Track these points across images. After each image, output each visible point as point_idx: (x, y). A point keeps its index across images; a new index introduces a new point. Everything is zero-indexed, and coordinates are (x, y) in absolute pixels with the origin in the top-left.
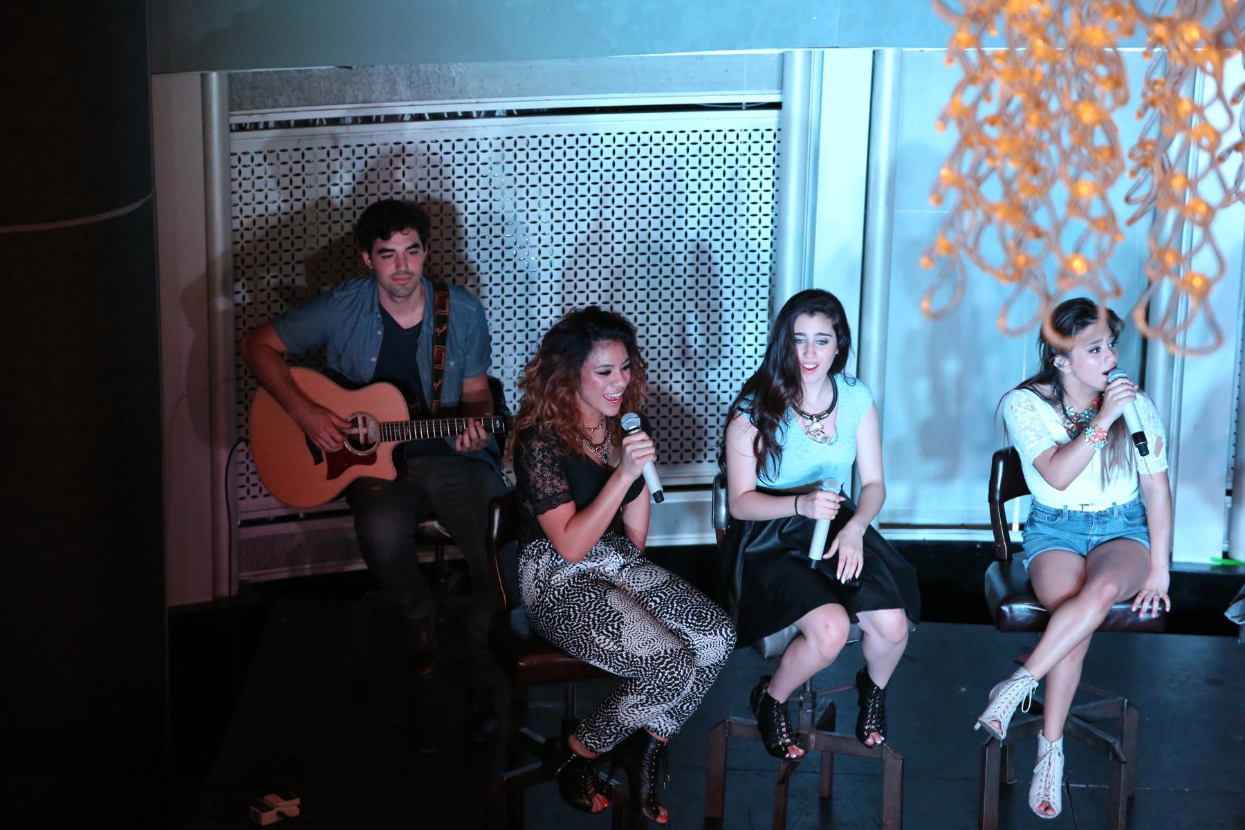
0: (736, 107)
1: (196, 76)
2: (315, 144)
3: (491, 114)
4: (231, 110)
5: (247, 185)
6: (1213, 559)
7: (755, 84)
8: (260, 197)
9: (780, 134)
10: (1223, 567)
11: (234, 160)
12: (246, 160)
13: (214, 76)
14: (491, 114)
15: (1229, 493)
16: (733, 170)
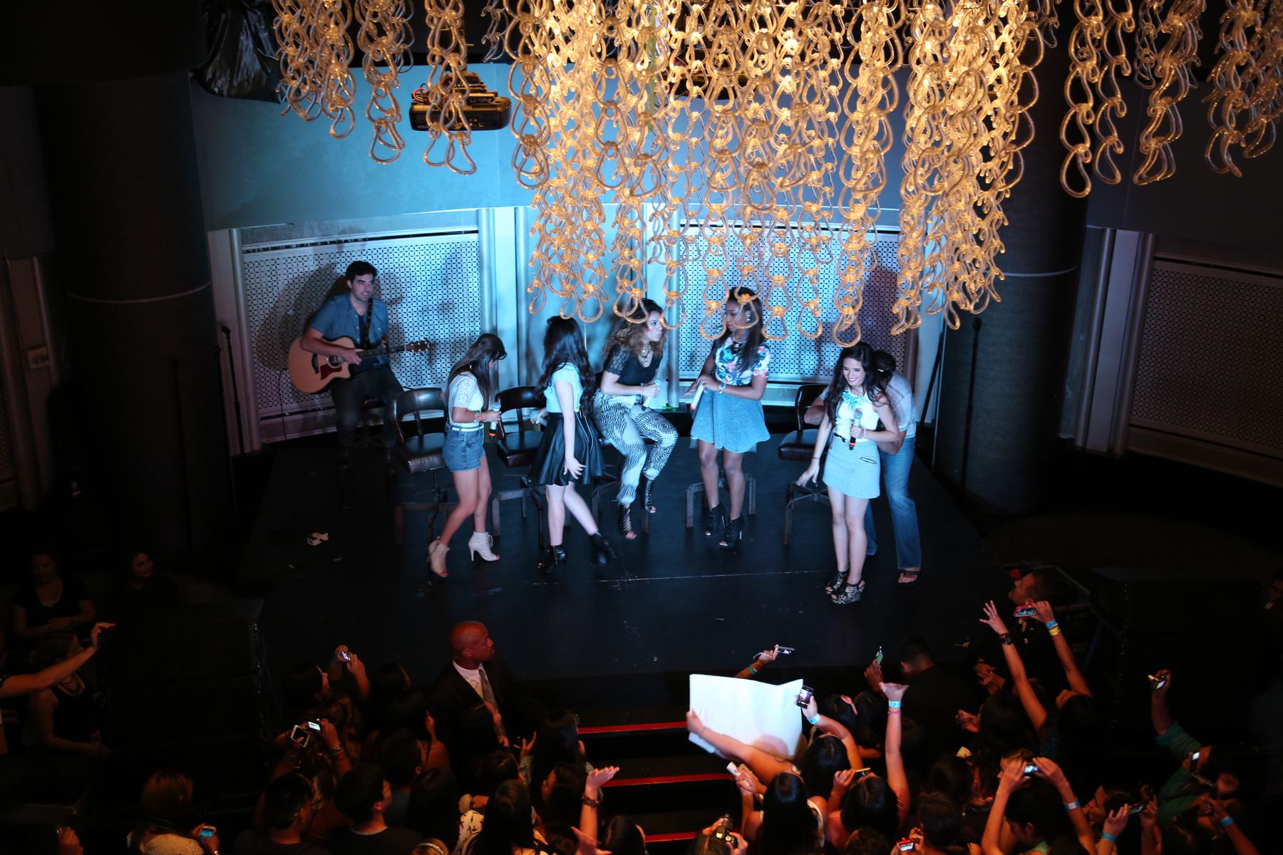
0: (460, 233)
1: (226, 231)
2: (280, 257)
3: (356, 240)
4: (243, 244)
5: (252, 276)
7: (466, 224)
8: (258, 280)
10: (667, 410)
11: (246, 266)
12: (251, 265)
13: (235, 231)
14: (356, 240)
15: (667, 380)
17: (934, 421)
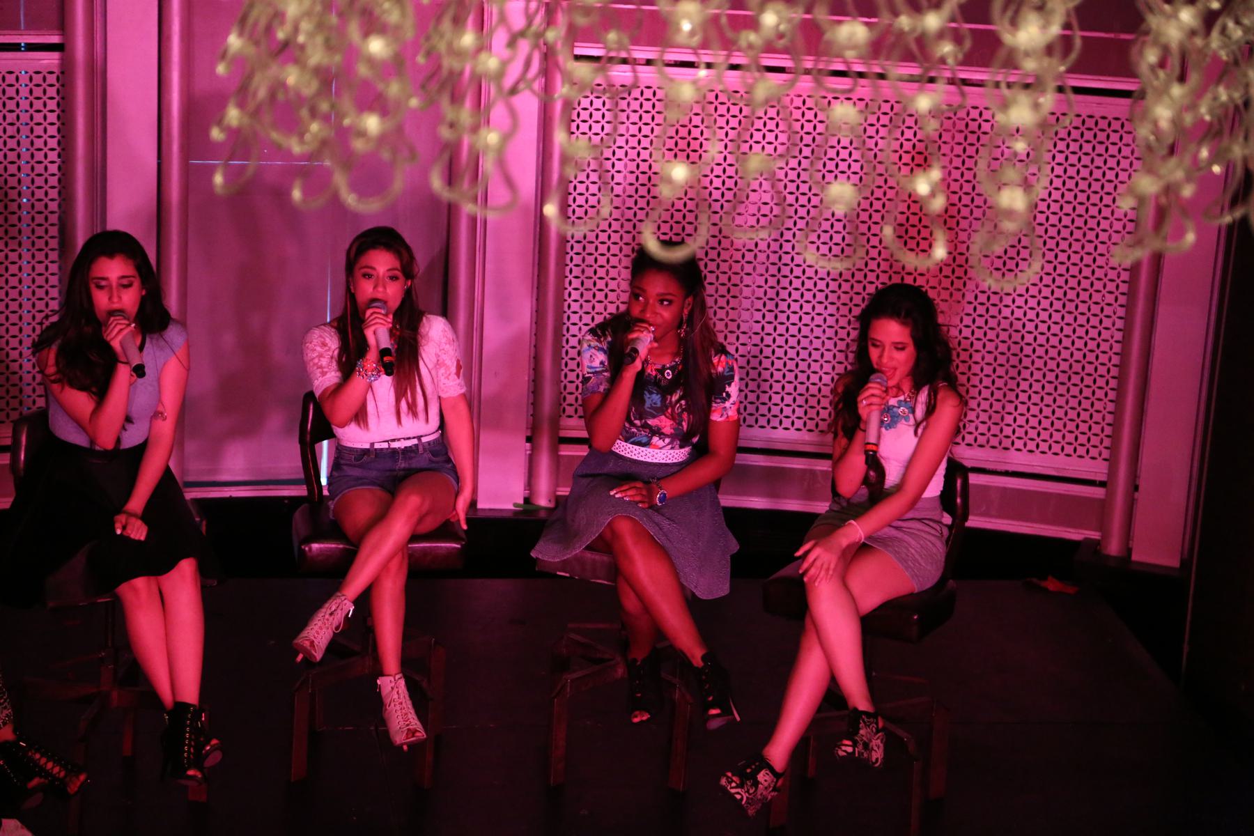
0: (15, 47)
6: (515, 505)
9: (65, 75)
10: (525, 512)
15: (529, 439)
16: (14, 115)
17: (1185, 564)
